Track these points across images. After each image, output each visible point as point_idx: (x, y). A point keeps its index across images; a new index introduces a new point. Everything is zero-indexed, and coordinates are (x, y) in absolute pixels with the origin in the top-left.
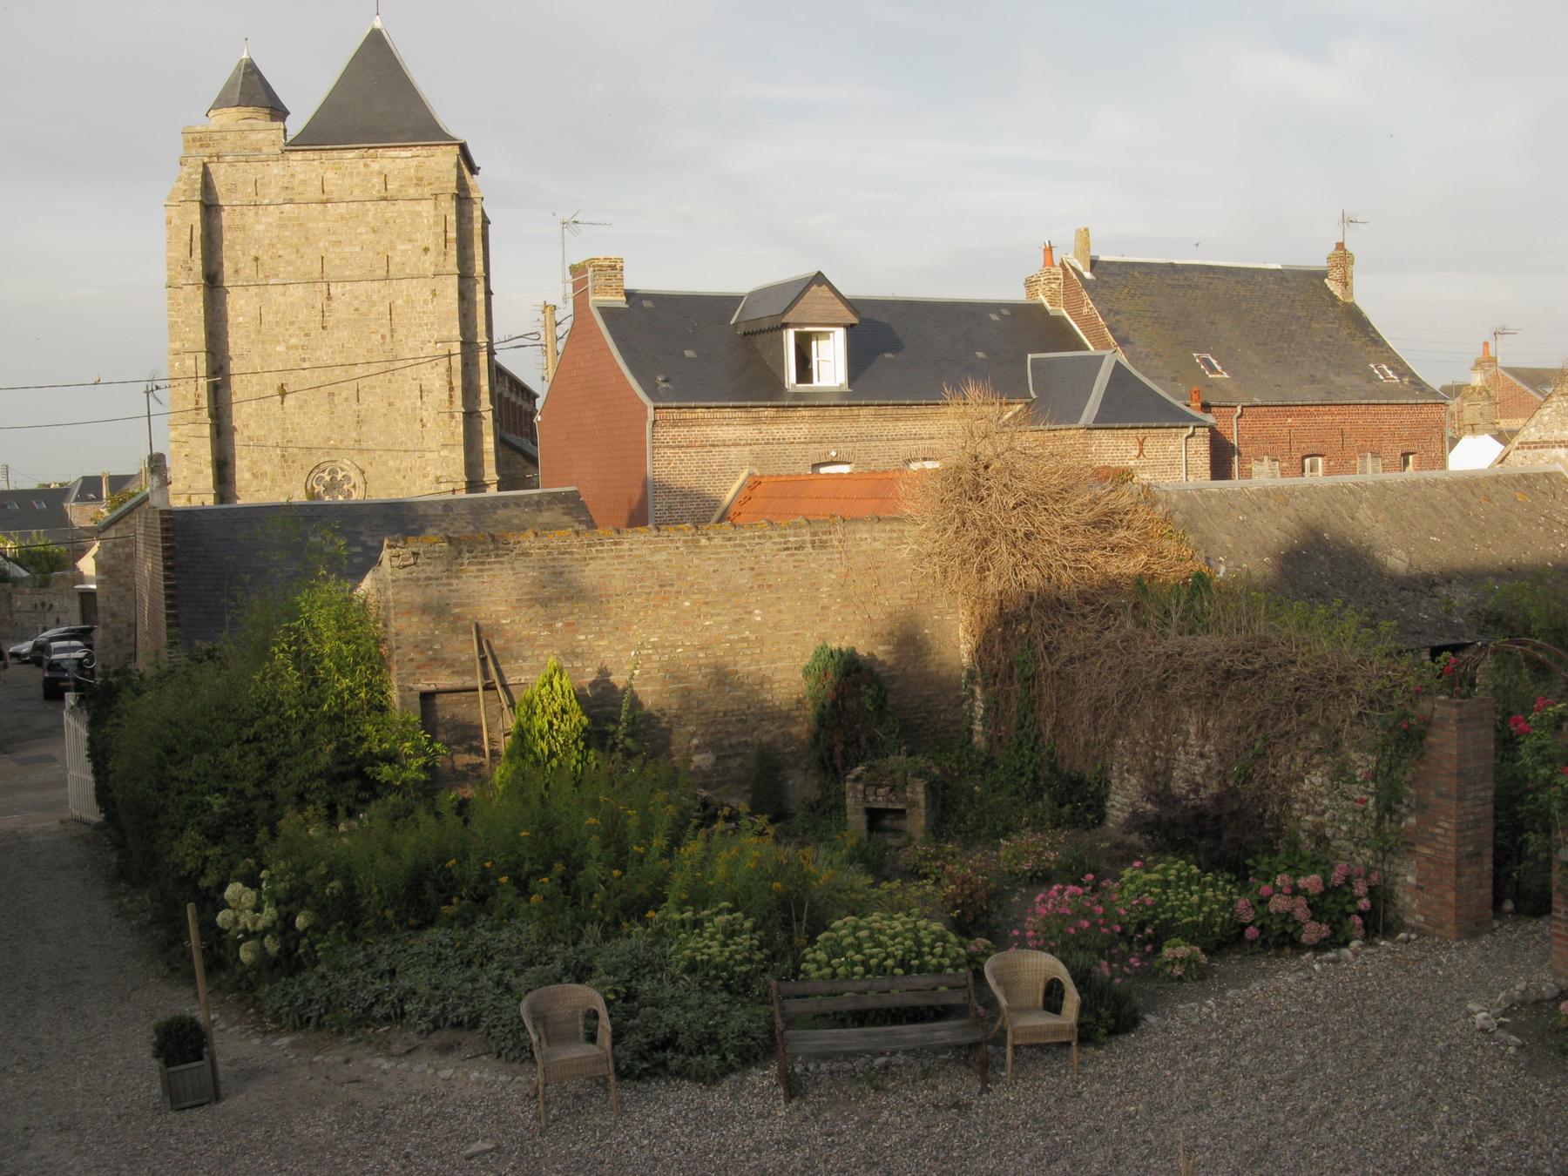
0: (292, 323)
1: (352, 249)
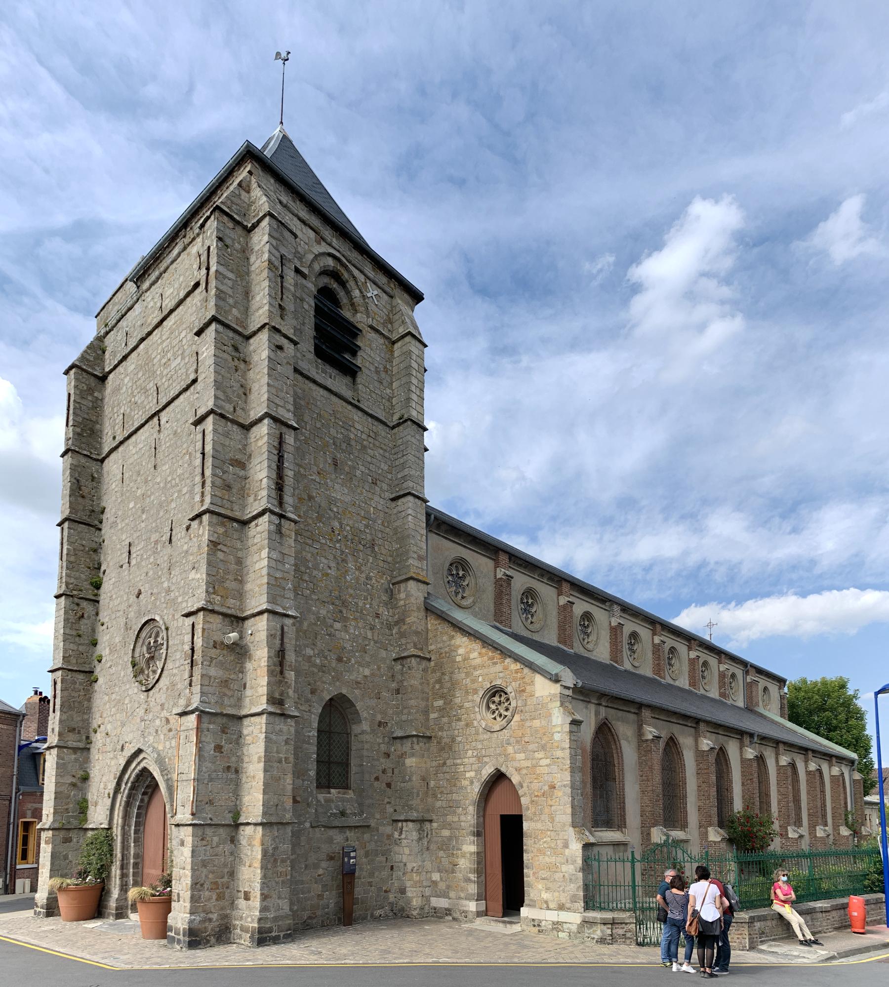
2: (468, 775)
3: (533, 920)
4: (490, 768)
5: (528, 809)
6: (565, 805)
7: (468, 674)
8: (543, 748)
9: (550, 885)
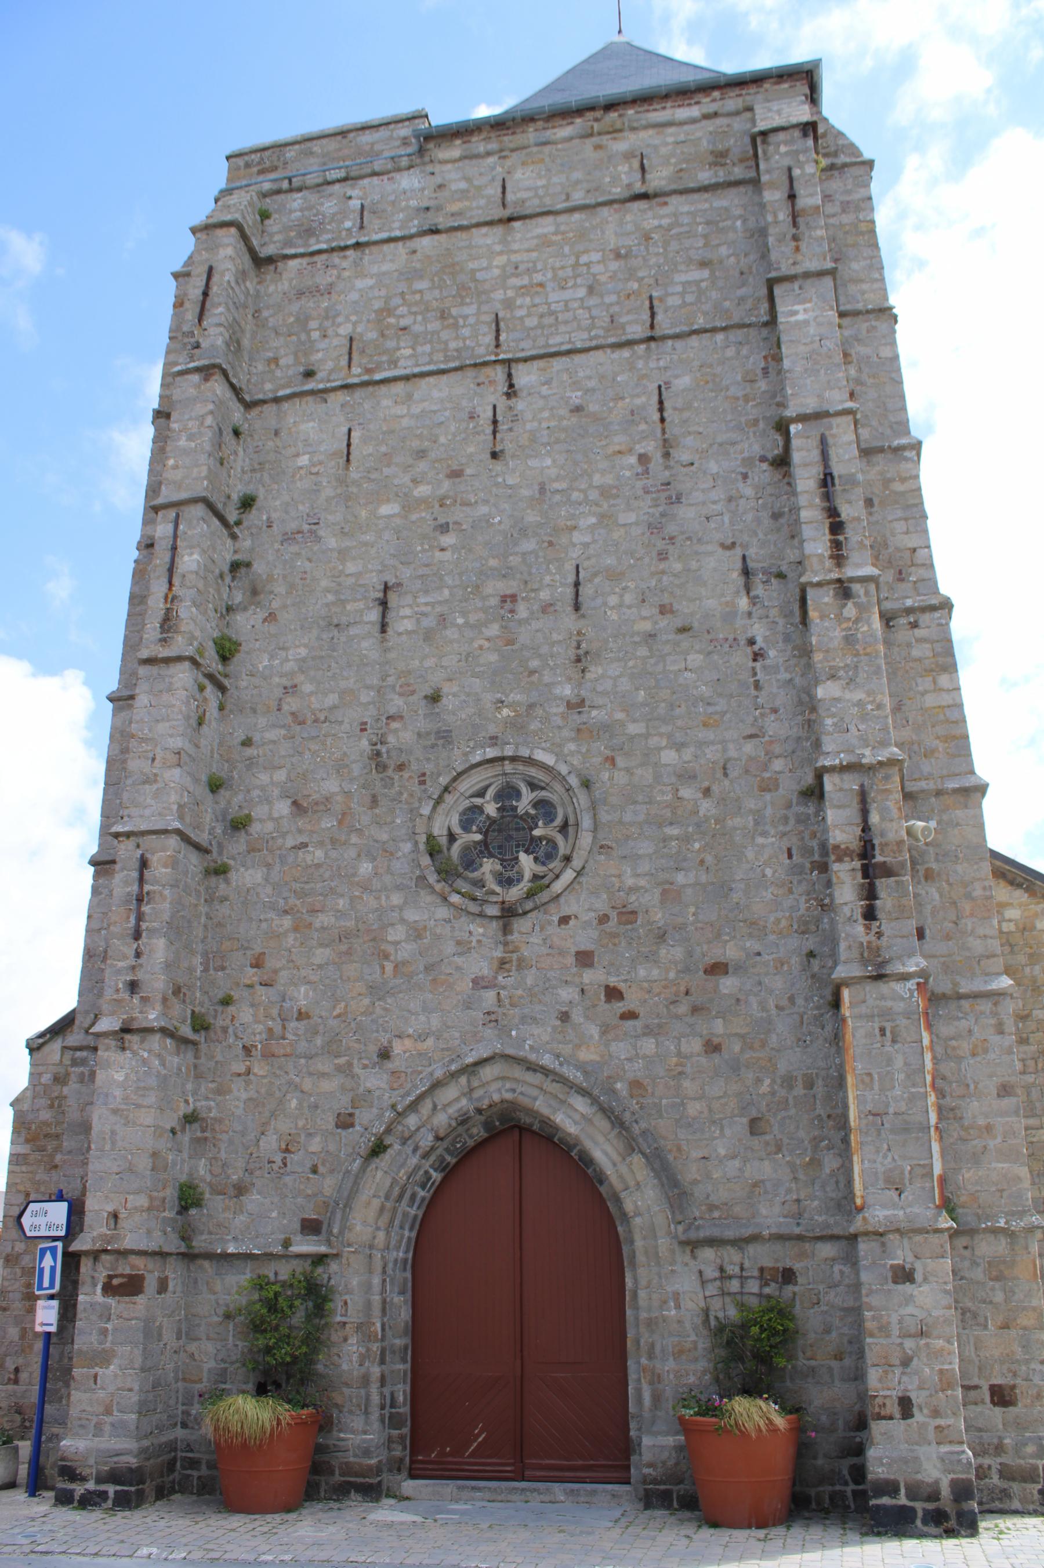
0: (421, 454)
1: (567, 294)
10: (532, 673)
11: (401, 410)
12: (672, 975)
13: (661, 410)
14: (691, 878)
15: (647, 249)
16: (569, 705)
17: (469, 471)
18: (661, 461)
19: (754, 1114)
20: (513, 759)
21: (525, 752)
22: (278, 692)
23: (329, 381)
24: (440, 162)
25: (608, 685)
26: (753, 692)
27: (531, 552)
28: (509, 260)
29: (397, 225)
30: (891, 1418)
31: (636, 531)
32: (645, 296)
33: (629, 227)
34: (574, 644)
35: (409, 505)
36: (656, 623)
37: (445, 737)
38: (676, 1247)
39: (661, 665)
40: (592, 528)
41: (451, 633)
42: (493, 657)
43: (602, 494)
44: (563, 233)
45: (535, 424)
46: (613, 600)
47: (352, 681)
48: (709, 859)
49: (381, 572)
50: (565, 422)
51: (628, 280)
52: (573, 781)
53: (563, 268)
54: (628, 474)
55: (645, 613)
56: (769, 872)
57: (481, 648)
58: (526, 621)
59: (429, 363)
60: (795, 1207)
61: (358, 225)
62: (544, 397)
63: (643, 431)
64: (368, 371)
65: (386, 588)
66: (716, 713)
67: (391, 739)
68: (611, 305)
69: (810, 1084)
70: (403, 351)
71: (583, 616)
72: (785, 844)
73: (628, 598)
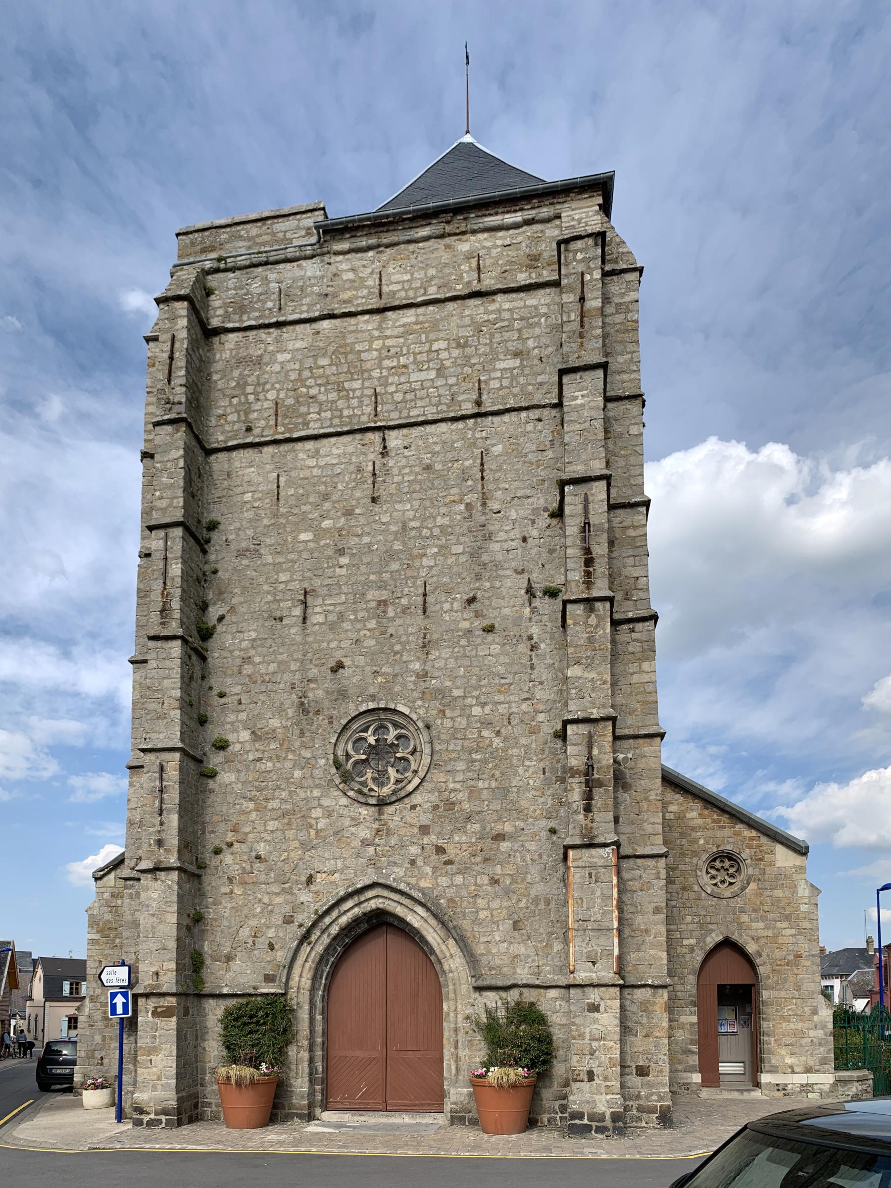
0: (326, 497)
1: (423, 376)
2: (686, 942)
3: (778, 1085)
4: (717, 935)
5: (768, 977)
6: (813, 973)
7: (682, 835)
8: (787, 918)
9: (796, 1050)
10: (396, 653)
11: (312, 462)
12: (473, 840)
13: (482, 471)
14: (486, 784)
15: (478, 339)
16: (418, 676)
17: (357, 511)
18: (480, 508)
19: (516, 918)
20: (385, 709)
21: (392, 706)
22: (238, 661)
23: (262, 436)
24: (335, 254)
25: (441, 663)
26: (529, 671)
27: (396, 571)
28: (384, 343)
29: (305, 308)
30: (582, 1081)
31: (463, 559)
32: (476, 379)
33: (467, 321)
34: (422, 635)
35: (319, 534)
36: (472, 623)
37: (342, 695)
38: (471, 989)
39: (474, 651)
40: (435, 555)
41: (346, 626)
42: (372, 642)
43: (441, 532)
44: (421, 323)
45: (400, 477)
46: (447, 606)
47: (285, 655)
48: (497, 774)
49: (302, 580)
50: (419, 477)
51: (465, 365)
52: (420, 724)
53: (420, 353)
54: (458, 517)
55: (466, 616)
56: (531, 782)
57: (365, 636)
58: (393, 619)
59: (329, 427)
60: (536, 970)
61: (277, 306)
62: (406, 457)
63: (470, 486)
64: (290, 431)
65: (306, 593)
66: (507, 684)
67: (310, 694)
68: (452, 385)
69: (548, 903)
70: (312, 415)
71: (428, 617)
72: (542, 765)
73: (456, 606)
